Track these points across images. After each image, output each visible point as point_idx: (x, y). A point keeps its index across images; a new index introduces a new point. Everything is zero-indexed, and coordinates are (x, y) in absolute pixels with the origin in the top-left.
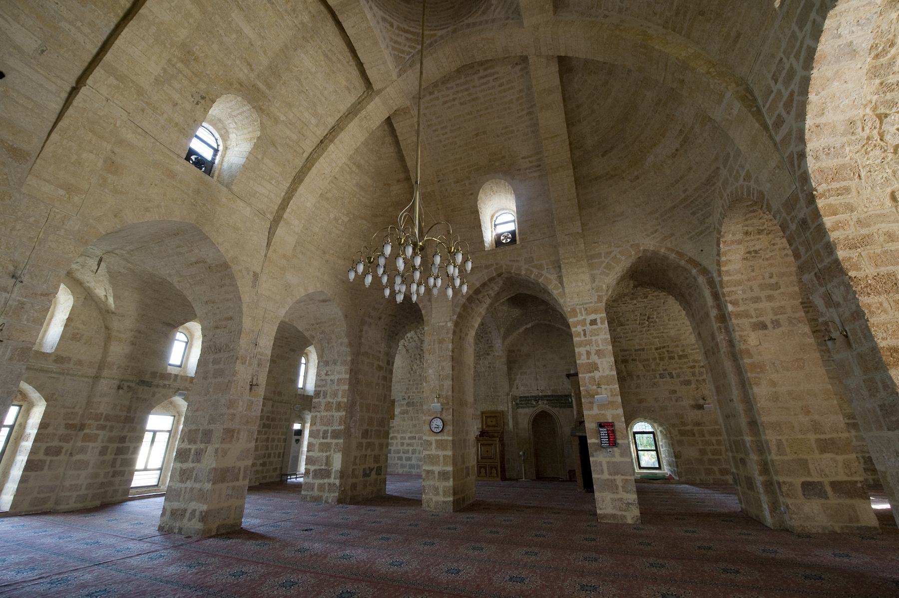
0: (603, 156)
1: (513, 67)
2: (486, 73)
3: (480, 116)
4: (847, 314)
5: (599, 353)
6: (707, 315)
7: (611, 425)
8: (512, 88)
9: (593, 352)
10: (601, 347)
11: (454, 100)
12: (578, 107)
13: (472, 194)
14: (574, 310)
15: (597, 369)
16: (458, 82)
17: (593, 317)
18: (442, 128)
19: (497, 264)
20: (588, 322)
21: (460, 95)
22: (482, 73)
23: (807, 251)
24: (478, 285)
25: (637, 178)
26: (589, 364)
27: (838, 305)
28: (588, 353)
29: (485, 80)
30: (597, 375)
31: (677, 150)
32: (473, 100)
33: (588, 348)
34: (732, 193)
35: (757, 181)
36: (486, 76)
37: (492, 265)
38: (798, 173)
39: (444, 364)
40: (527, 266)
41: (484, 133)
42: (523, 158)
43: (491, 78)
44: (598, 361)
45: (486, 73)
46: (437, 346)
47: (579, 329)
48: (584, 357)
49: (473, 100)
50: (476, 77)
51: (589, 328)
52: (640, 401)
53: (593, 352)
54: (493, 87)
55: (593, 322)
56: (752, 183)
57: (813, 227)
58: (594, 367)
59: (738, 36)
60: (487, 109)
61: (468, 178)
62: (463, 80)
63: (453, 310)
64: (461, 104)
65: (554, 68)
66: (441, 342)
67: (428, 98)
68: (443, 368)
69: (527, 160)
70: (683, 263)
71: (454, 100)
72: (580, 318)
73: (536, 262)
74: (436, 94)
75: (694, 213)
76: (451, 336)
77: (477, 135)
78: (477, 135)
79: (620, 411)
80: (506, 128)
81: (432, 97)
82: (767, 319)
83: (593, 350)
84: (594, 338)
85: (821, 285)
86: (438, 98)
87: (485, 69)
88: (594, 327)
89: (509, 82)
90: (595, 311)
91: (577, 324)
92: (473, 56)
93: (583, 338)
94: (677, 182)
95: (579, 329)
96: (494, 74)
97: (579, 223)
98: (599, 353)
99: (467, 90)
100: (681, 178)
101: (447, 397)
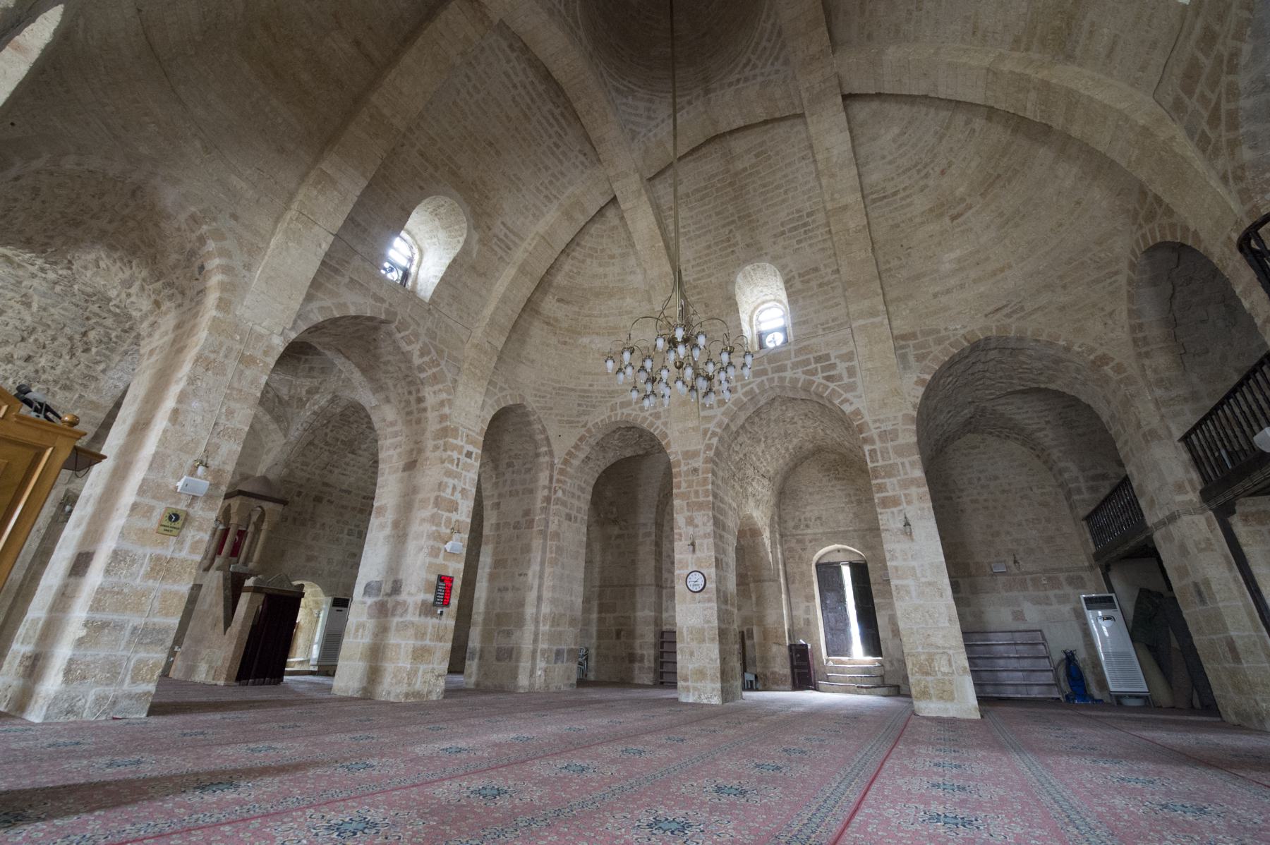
0: (559, 300)
1: (580, 151)
2: (559, 117)
3: (513, 136)
4: (701, 533)
5: (463, 491)
6: (531, 491)
7: (451, 580)
8: (561, 162)
9: (459, 489)
10: (467, 487)
11: (515, 86)
12: (578, 244)
13: (421, 188)
14: (456, 430)
15: (456, 510)
16: (536, 82)
17: (471, 448)
18: (475, 87)
19: (391, 305)
20: (465, 452)
21: (523, 93)
22: (557, 112)
23: (689, 487)
24: (352, 312)
25: (565, 343)
26: (452, 501)
27: (697, 526)
28: (454, 488)
29: (552, 120)
30: (455, 517)
32: (525, 115)
33: (456, 482)
34: (630, 415)
35: (665, 424)
36: (557, 120)
37: (382, 300)
38: (707, 441)
39: (233, 405)
40: (427, 340)
41: (498, 153)
42: (503, 223)
43: (556, 128)
44: (460, 502)
45: (559, 117)
46: (231, 365)
47: (455, 455)
48: (449, 491)
49: (525, 115)
50: (550, 106)
51: (463, 459)
52: (309, 559)
53: (459, 489)
54: (550, 137)
55: (469, 455)
56: (659, 423)
57: (701, 476)
58: (453, 507)
60: (524, 139)
61: (436, 168)
62: (541, 88)
63: (295, 322)
64: (514, 99)
65: (602, 203)
66: (246, 360)
67: (504, 45)
68: (230, 413)
69: (505, 230)
70: (540, 437)
71: (515, 86)
72: (459, 442)
73: (437, 343)
74: (513, 56)
75: (579, 405)
76: (272, 362)
77: (491, 144)
78: (491, 144)
79: (461, 566)
80: (519, 179)
81: (508, 51)
82: (574, 513)
83: (460, 485)
84: (464, 473)
86: (508, 61)
87: (562, 115)
88: (468, 460)
89: (564, 154)
90: (472, 443)
91: (454, 448)
92: (579, 99)
93: (454, 468)
94: (590, 373)
95: (455, 455)
96: (562, 128)
97: (504, 339)
98: (463, 491)
99: (532, 100)
101: (218, 473)
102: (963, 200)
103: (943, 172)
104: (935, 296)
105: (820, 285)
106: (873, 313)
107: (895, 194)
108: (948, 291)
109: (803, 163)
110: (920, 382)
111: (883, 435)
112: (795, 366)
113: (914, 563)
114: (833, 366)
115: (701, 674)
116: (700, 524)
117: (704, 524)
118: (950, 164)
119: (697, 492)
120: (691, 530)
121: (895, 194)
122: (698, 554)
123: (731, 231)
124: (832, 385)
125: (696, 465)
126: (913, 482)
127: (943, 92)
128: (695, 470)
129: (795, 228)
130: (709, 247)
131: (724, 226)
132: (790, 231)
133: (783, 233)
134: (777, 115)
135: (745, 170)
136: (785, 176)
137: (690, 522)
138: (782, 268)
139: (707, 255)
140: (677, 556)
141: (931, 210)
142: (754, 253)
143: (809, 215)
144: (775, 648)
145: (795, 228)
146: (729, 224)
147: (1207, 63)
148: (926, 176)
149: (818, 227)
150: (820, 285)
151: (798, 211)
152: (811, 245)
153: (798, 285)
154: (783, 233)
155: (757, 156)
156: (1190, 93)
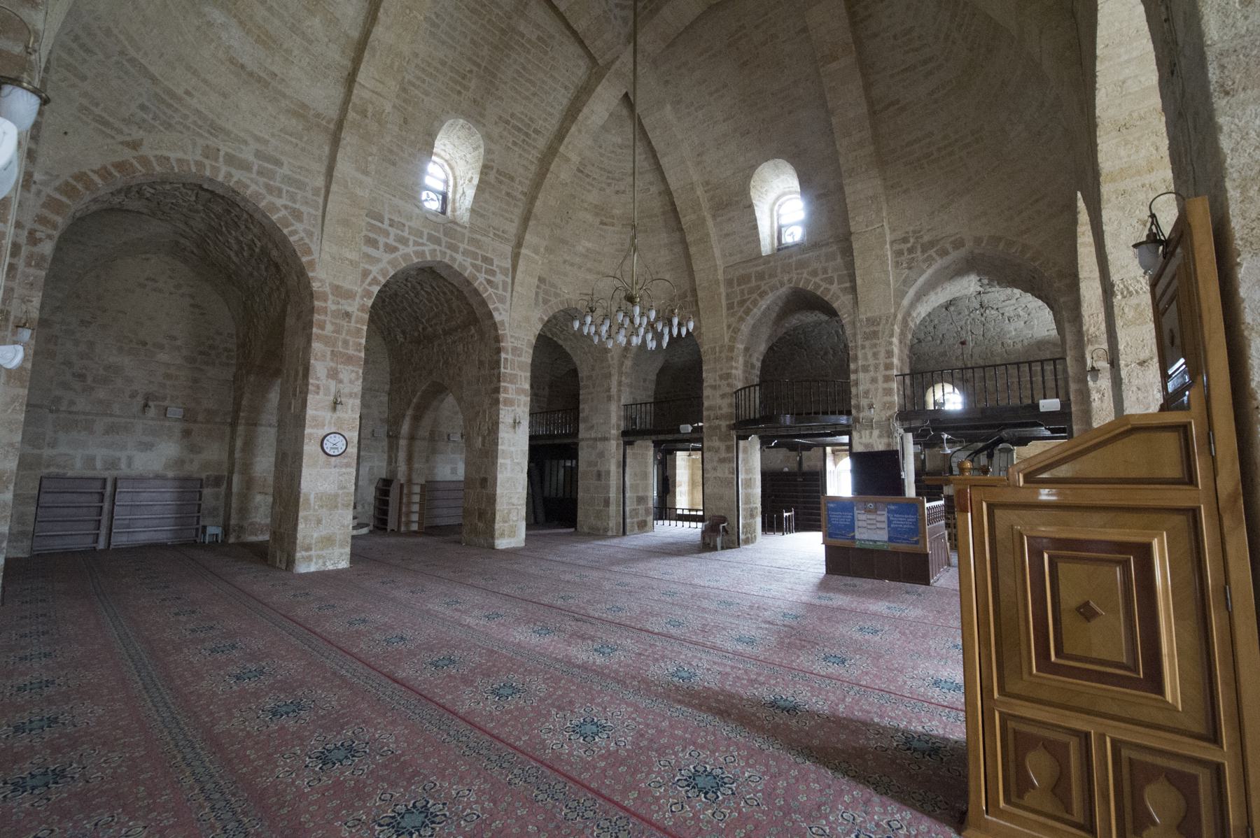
27: (341, 382)
31: (242, 66)
57: (353, 324)
59: (394, 164)
85: (332, 360)
100: (205, 81)
102: (613, 217)
103: (617, 192)
104: (565, 262)
105: (508, 194)
106: (536, 251)
107: (588, 176)
108: (572, 265)
109: (563, 91)
110: (541, 319)
111: (515, 349)
112: (465, 253)
113: (512, 449)
114: (493, 273)
115: (328, 541)
116: (346, 380)
117: (351, 382)
118: (624, 192)
119: (346, 342)
120: (332, 385)
121: (588, 176)
122: (338, 414)
123: (471, 72)
124: (490, 290)
125: (349, 309)
126: (523, 391)
127: (664, 162)
128: (347, 315)
129: (519, 130)
130: (443, 63)
131: (469, 59)
132: (514, 127)
133: (507, 122)
134: (587, 42)
135: (523, 36)
136: (544, 82)
137: (333, 374)
138: (488, 151)
139: (436, 69)
140: (310, 412)
141: (596, 206)
142: (475, 115)
143: (536, 131)
144: (259, 498)
145: (519, 130)
146: (475, 63)
147: (753, 283)
148: (609, 185)
149: (535, 147)
150: (508, 194)
151: (531, 119)
152: (520, 156)
153: (492, 177)
154: (507, 122)
155: (539, 38)
156: (739, 285)
